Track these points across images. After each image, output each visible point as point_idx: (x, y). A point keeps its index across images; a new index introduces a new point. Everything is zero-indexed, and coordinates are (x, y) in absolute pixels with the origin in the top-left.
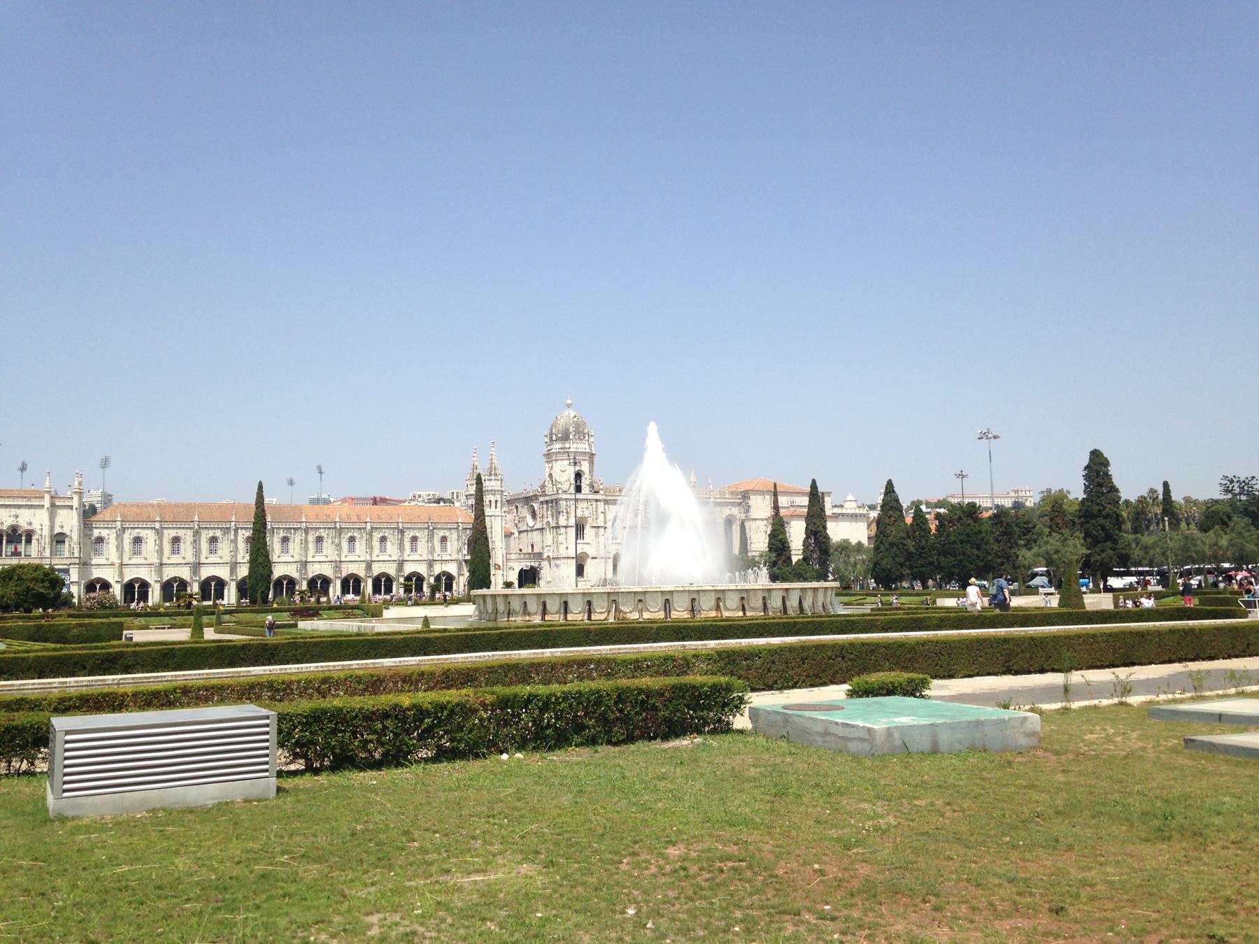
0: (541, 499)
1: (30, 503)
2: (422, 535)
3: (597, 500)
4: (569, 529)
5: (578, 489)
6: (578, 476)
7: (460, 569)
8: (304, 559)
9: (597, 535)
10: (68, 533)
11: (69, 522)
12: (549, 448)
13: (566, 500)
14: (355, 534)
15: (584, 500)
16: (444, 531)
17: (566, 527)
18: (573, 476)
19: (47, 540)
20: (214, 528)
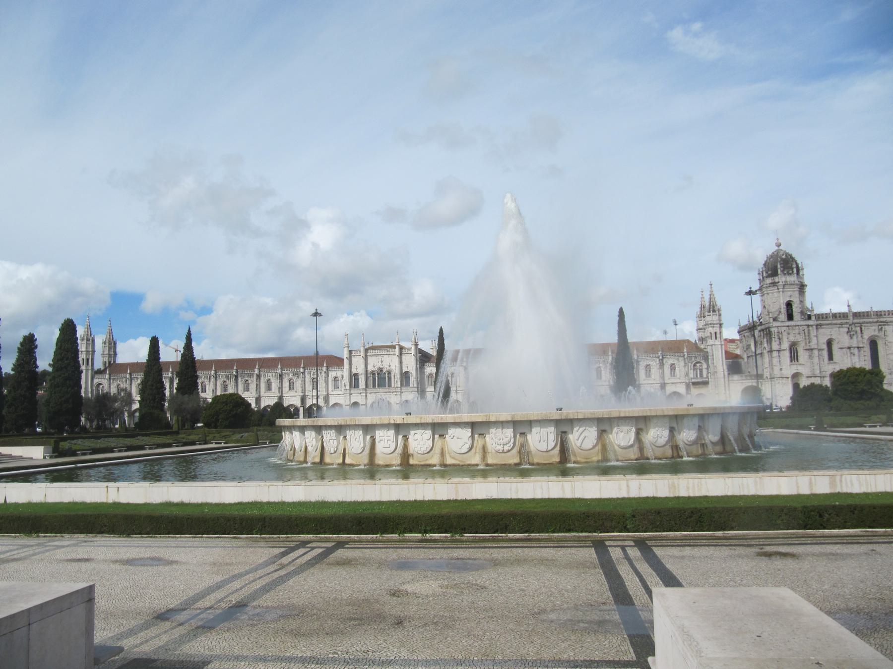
0: (759, 328)
1: (389, 353)
2: (654, 364)
3: (808, 326)
4: (782, 352)
5: (790, 317)
6: (789, 305)
8: (663, 382)
9: (811, 357)
10: (411, 371)
11: (410, 363)
12: (762, 284)
14: (601, 365)
15: (796, 326)
17: (779, 351)
19: (398, 376)
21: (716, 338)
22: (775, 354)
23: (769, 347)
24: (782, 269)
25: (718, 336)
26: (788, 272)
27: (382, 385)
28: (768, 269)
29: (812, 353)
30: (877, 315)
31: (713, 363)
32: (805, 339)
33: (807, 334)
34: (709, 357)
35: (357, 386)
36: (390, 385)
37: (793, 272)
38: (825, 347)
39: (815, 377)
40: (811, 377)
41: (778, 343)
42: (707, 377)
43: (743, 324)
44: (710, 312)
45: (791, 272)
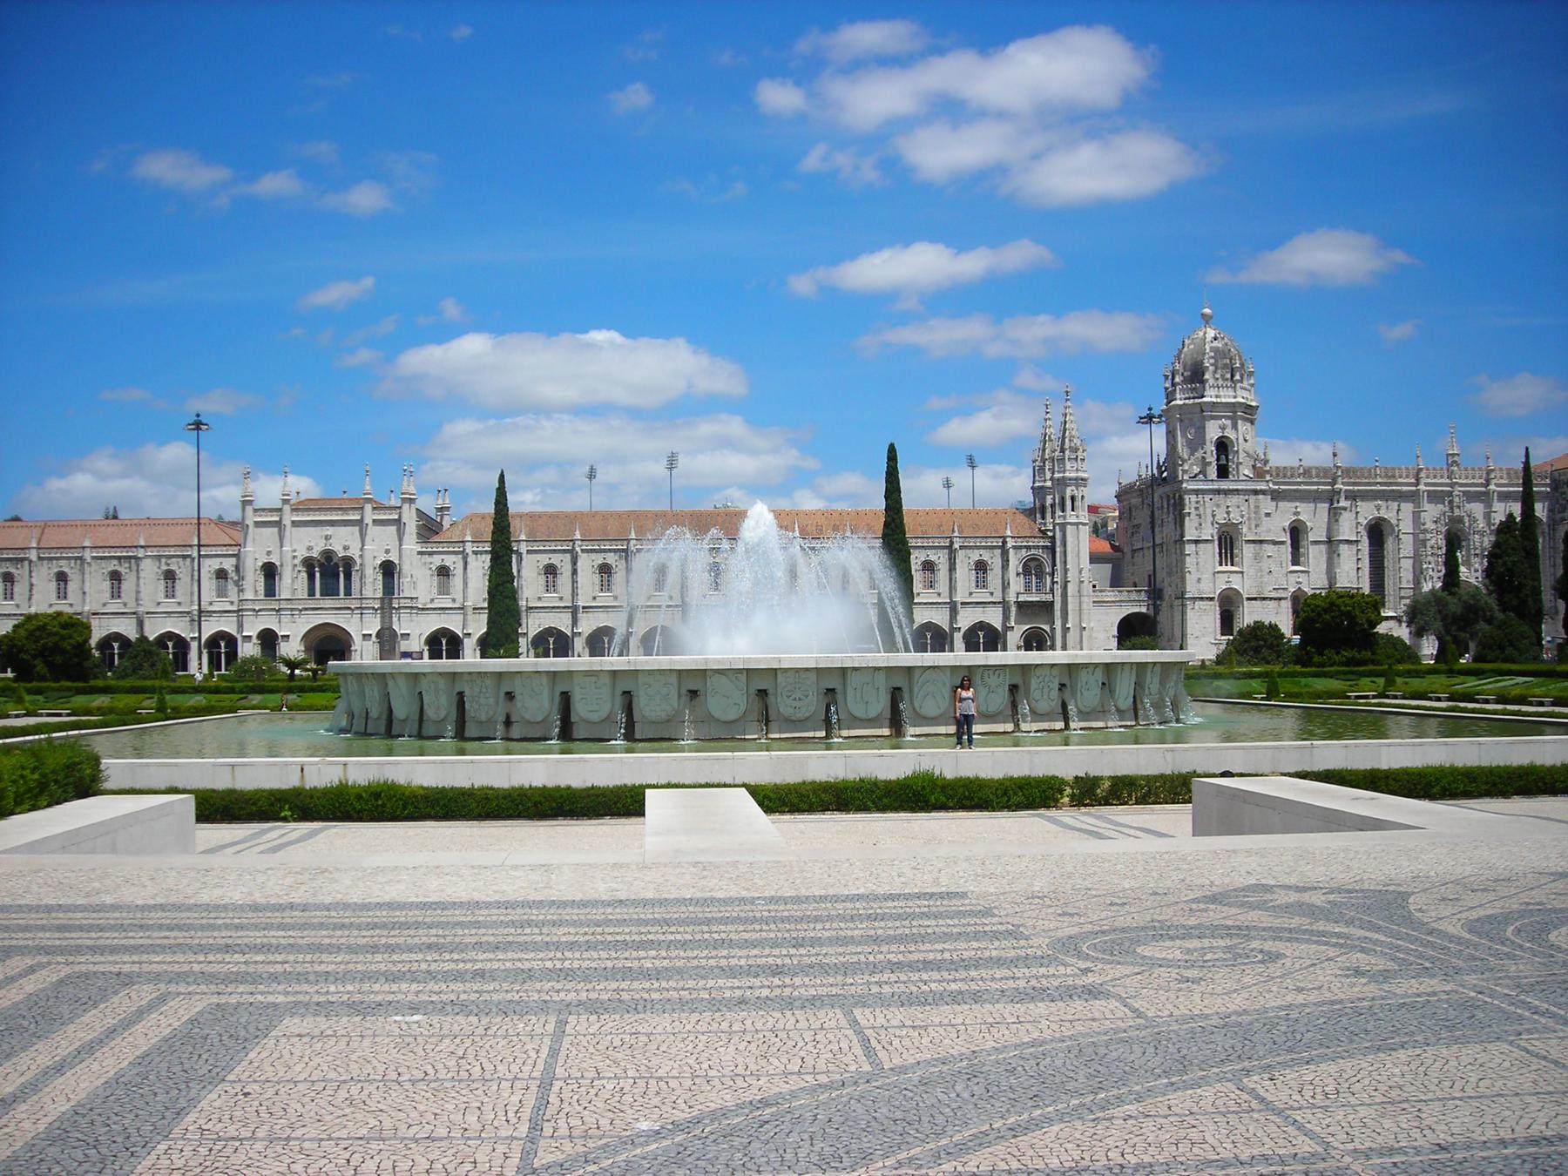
3: (1256, 492)
5: (1223, 472)
7: (1006, 617)
9: (1257, 557)
13: (1197, 492)
16: (982, 552)
17: (1196, 542)
18: (1211, 448)
20: (605, 551)
21: (1073, 510)
22: (1189, 549)
23: (1178, 532)
24: (1211, 368)
25: (1076, 504)
26: (1222, 376)
27: (330, 591)
28: (1184, 368)
29: (1261, 549)
30: (1387, 476)
31: (1065, 562)
32: (1249, 519)
33: (1252, 506)
34: (1058, 550)
35: (270, 591)
36: (348, 592)
37: (1232, 376)
38: (1287, 538)
39: (1264, 599)
40: (1255, 599)
41: (1197, 525)
42: (1052, 590)
43: (1125, 482)
44: (1063, 451)
45: (1229, 376)
